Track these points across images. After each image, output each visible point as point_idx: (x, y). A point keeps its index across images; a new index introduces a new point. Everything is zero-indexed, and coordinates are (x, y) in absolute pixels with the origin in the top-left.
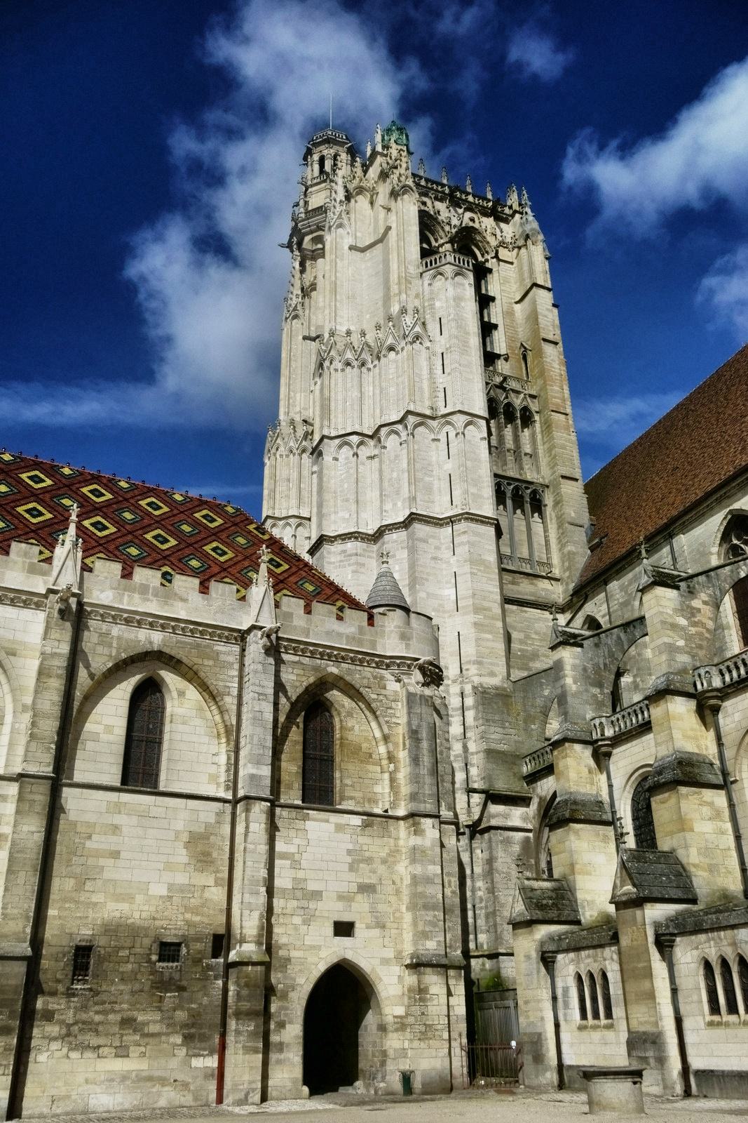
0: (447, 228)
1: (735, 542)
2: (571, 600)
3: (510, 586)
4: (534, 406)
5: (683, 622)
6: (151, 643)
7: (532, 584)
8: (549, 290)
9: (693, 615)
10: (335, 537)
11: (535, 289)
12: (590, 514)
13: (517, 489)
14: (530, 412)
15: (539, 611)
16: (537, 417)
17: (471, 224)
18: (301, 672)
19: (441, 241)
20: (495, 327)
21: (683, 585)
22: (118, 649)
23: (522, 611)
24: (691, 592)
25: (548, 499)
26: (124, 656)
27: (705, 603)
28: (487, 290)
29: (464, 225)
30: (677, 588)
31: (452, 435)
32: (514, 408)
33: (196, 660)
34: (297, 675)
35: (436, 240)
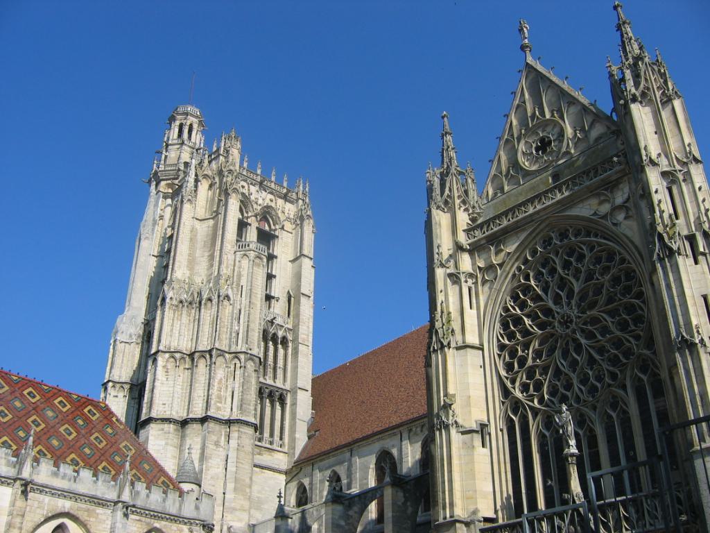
0: (255, 206)
1: (382, 464)
2: (292, 469)
3: (258, 456)
4: (290, 337)
5: (343, 523)
6: (64, 507)
7: (271, 455)
8: (311, 259)
9: (348, 519)
10: (158, 419)
11: (302, 257)
12: (312, 409)
13: (271, 392)
14: (287, 340)
15: (272, 472)
16: (290, 344)
17: (270, 204)
18: (140, 526)
19: (250, 214)
20: (275, 277)
21: (347, 502)
22: (47, 511)
23: (262, 472)
24: (349, 507)
25: (288, 401)
26: (50, 515)
27: (355, 512)
28: (273, 250)
29: (265, 204)
30: (343, 504)
31: (238, 365)
32: (277, 337)
33: (86, 518)
34: (138, 528)
35: (247, 213)
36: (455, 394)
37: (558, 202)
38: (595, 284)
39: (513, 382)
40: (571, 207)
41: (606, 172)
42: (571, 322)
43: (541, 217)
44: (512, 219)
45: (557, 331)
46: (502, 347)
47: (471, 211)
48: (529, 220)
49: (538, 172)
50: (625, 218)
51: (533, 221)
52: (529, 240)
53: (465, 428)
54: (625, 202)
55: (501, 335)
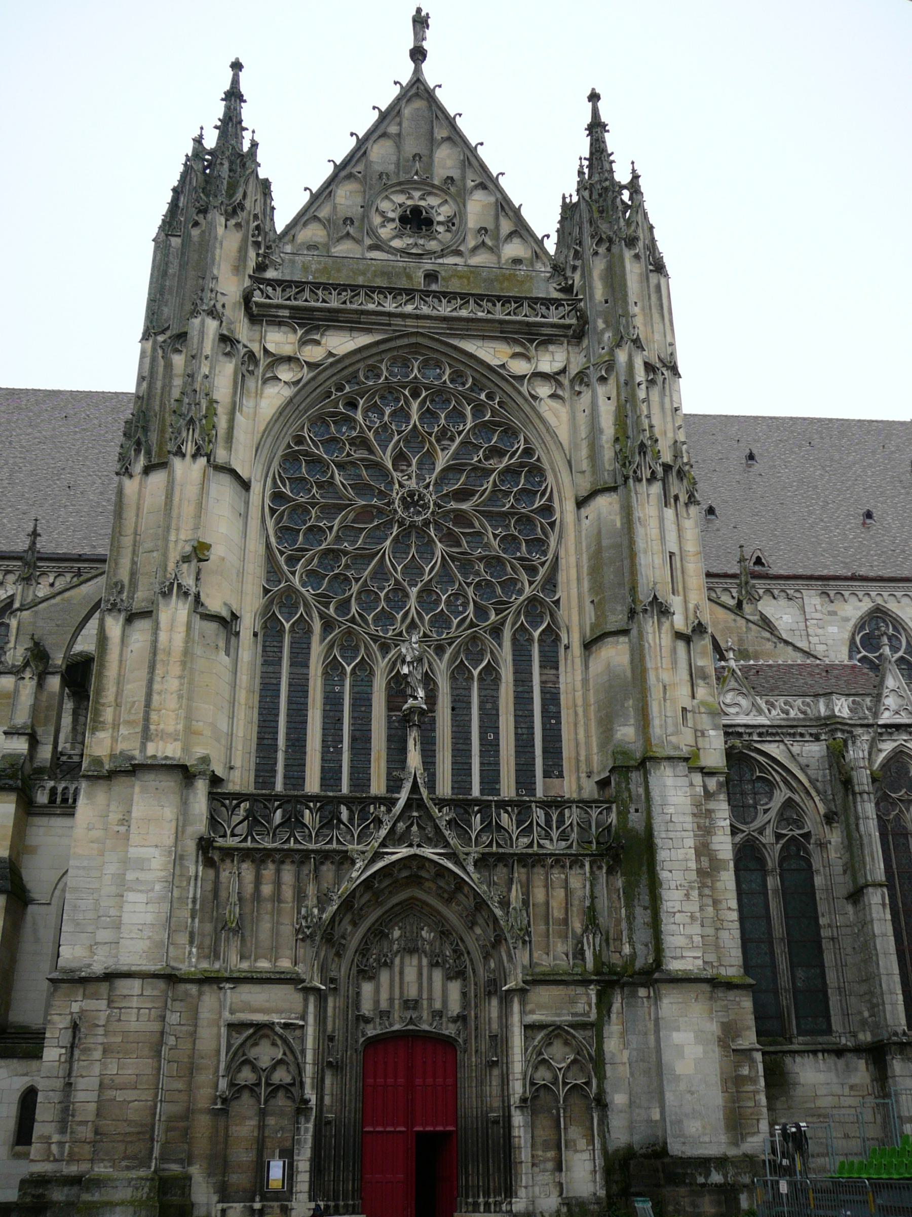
36: (210, 546)
37: (445, 319)
38: (475, 469)
39: (292, 561)
40: (462, 337)
41: (537, 315)
42: (425, 507)
43: (406, 326)
44: (351, 302)
45: (395, 511)
46: (278, 497)
47: (261, 252)
48: (385, 320)
49: (403, 252)
50: (553, 396)
51: (390, 325)
52: (374, 350)
53: (206, 607)
54: (558, 373)
55: (280, 476)
